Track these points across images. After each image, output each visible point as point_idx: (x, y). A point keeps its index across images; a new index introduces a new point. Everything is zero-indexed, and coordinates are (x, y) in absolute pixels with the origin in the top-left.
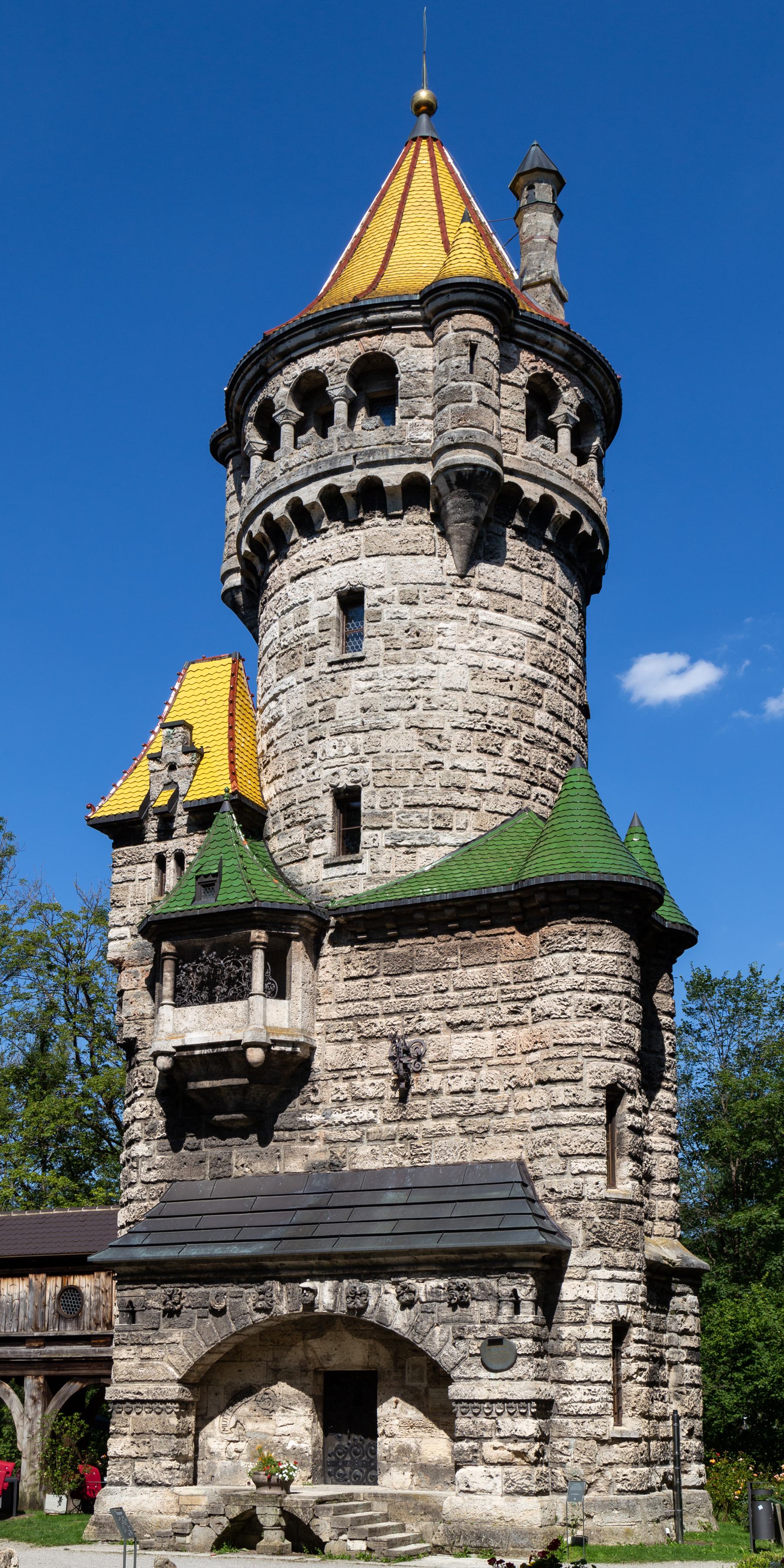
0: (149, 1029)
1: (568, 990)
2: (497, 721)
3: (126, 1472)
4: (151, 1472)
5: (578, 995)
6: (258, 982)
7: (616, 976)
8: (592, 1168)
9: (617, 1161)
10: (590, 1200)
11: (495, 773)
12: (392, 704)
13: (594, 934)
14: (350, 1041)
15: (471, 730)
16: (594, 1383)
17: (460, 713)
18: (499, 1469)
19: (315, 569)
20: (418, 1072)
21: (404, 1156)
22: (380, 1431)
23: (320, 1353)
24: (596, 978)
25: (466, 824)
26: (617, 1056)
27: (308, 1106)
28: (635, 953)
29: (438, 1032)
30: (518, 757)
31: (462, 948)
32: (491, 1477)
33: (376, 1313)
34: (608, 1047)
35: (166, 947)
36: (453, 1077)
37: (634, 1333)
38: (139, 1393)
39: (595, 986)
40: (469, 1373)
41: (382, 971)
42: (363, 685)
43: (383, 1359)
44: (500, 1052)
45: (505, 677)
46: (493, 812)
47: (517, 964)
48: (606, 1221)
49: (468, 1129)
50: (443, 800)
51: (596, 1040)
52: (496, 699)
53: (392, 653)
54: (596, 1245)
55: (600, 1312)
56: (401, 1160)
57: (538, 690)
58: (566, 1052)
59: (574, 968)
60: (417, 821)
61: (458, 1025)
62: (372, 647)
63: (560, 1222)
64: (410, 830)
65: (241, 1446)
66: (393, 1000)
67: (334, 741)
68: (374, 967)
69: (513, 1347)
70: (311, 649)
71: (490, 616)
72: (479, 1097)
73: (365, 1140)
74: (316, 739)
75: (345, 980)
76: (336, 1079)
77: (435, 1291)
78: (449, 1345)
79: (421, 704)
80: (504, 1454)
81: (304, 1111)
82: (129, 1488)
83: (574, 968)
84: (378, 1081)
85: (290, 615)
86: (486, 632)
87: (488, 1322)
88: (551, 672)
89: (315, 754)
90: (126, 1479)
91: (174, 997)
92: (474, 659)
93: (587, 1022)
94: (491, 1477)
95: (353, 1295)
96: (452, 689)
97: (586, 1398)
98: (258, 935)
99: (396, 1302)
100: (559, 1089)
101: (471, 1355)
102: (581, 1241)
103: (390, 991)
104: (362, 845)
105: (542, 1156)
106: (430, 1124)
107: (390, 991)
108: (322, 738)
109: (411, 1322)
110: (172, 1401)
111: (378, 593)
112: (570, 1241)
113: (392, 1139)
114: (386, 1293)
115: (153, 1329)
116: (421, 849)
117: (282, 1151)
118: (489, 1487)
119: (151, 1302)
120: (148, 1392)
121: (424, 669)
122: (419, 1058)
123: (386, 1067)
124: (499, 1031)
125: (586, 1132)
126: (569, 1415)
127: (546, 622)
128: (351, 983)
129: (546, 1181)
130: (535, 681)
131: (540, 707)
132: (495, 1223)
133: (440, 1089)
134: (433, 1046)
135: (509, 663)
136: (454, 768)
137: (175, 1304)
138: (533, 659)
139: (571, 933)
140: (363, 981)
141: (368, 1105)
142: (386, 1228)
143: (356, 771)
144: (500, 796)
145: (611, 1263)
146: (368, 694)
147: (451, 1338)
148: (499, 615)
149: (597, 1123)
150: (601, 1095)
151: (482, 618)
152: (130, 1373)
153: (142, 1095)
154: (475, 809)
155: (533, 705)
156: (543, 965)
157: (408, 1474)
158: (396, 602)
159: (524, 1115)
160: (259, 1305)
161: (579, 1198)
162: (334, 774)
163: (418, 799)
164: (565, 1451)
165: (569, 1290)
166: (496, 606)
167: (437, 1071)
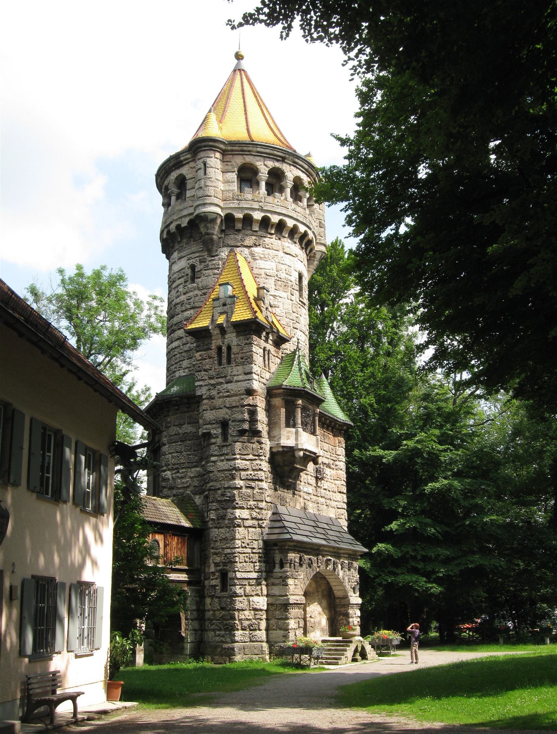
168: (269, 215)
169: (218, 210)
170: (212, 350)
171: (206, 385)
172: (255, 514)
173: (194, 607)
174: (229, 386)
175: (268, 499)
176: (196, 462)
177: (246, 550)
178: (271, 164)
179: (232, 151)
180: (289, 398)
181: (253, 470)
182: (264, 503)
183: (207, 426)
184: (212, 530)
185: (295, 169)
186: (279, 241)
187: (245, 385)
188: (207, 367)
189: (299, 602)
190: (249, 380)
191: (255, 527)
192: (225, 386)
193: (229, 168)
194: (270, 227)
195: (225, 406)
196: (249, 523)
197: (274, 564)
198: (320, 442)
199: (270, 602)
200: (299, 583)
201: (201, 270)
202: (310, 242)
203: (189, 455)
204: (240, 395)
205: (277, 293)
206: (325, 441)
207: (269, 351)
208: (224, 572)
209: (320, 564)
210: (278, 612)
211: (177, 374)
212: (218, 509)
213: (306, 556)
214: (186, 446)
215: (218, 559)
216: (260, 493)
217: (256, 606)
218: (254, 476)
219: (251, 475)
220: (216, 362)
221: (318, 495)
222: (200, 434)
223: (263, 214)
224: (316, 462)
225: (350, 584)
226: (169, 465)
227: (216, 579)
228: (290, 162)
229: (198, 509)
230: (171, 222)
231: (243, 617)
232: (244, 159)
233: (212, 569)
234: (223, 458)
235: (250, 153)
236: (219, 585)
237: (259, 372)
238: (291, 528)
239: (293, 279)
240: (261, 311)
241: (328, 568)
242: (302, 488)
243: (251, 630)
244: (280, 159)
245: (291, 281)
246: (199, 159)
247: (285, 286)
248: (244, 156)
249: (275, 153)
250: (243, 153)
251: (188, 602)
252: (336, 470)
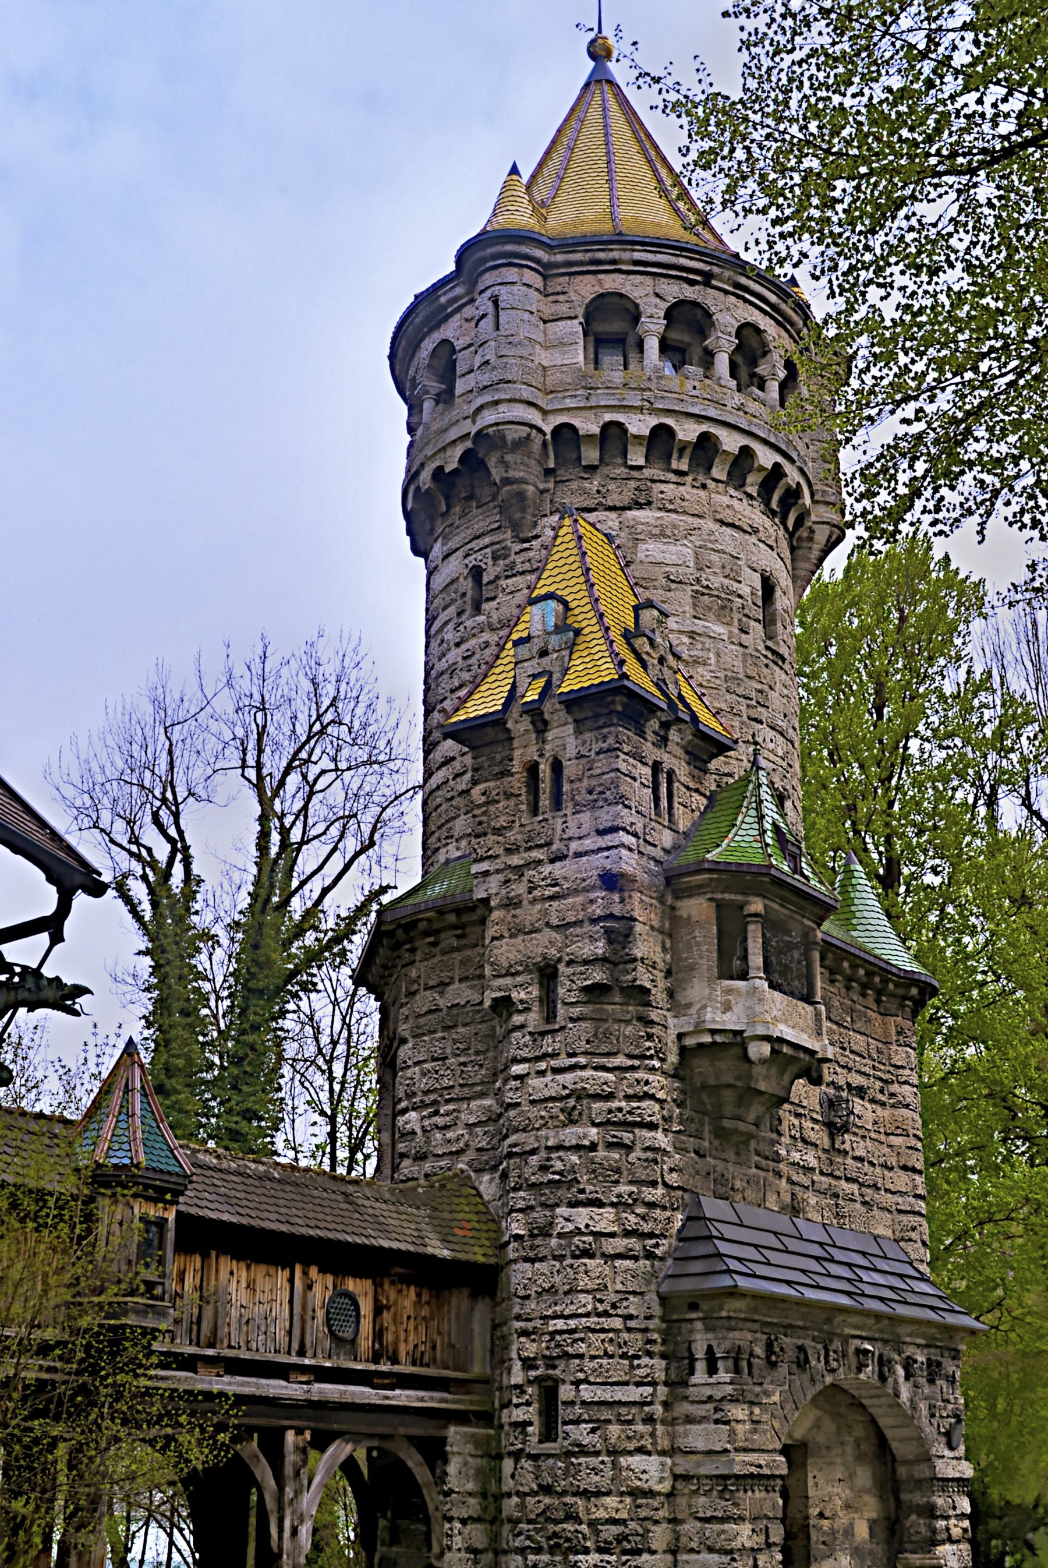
38: (760, 1466)
105: (910, 1240)
168: (670, 421)
169: (534, 416)
170: (512, 775)
171: (498, 871)
172: (633, 1219)
173: (470, 1486)
174: (558, 869)
175: (673, 1179)
176: (482, 1083)
177: (606, 1323)
178: (674, 291)
179: (569, 264)
180: (727, 896)
181: (628, 1098)
182: (660, 1191)
183: (501, 981)
184: (514, 1267)
185: (740, 303)
186: (702, 493)
187: (599, 861)
188: (502, 821)
189: (766, 1471)
190: (608, 848)
191: (636, 1258)
192: (547, 869)
193: (563, 309)
194: (675, 455)
195: (548, 925)
196: (619, 1244)
197: (692, 1360)
198: (826, 1024)
199: (679, 1470)
200: (765, 1417)
201: (497, 578)
202: (793, 495)
203: (464, 1064)
204: (586, 890)
205: (699, 625)
206: (857, 1026)
207: (671, 775)
208: (550, 1383)
209: (835, 1364)
210: (702, 1500)
211: (442, 857)
212: (531, 1208)
213: (788, 1340)
214: (455, 1041)
215: (531, 1349)
216: (646, 1160)
217: (639, 1483)
218: (630, 1113)
219: (620, 1110)
220: (524, 807)
221: (837, 1173)
222: (487, 1003)
223: (653, 421)
224: (817, 1081)
225: (935, 1421)
226: (414, 1094)
227: (528, 1404)
228: (726, 287)
229: (488, 1212)
230: (422, 465)
231: (601, 1514)
232: (600, 281)
233: (517, 1376)
234: (543, 1066)
235: (614, 267)
236: (536, 1423)
237: (639, 828)
238: (739, 1260)
239: (744, 590)
240: (644, 665)
241: (862, 1376)
242: (783, 1152)
243: (625, 1552)
244: (698, 278)
245: (740, 596)
246: (482, 292)
247: (723, 608)
248: (601, 276)
249: (683, 261)
250: (596, 268)
251: (452, 1469)
252: (893, 1106)
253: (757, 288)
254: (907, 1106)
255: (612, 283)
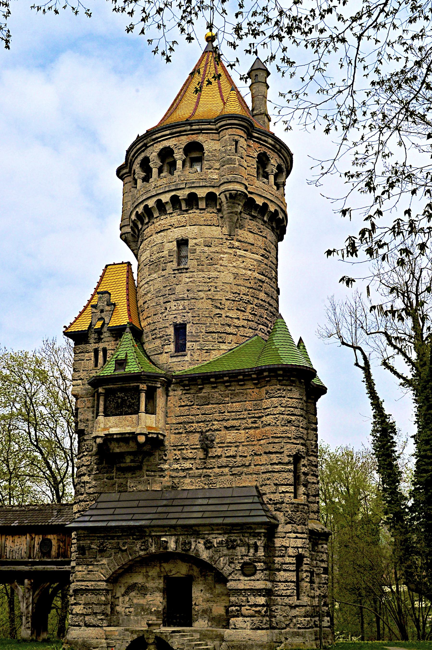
0: (90, 426)
1: (278, 414)
2: (244, 297)
3: (81, 621)
4: (92, 621)
5: (282, 416)
6: (143, 407)
7: (297, 408)
8: (287, 490)
9: (298, 487)
10: (287, 504)
11: (243, 319)
12: (200, 288)
13: (288, 390)
14: (181, 433)
15: (234, 301)
16: (288, 582)
17: (229, 293)
18: (248, 619)
19: (167, 229)
20: (212, 448)
21: (205, 484)
22: (193, 603)
23: (167, 569)
24: (289, 409)
25: (232, 341)
26: (298, 442)
27: (162, 461)
28: (305, 398)
29: (220, 430)
30: (253, 312)
31: (231, 395)
32: (245, 622)
33: (195, 551)
34: (294, 438)
35: (100, 390)
36: (227, 450)
37: (305, 561)
39: (289, 412)
40: (236, 577)
41: (196, 403)
42: (188, 280)
43: (196, 572)
44: (248, 440)
45: (247, 278)
46: (243, 336)
47: (255, 402)
48: (294, 513)
49: (234, 472)
50: (222, 330)
51: (290, 435)
52: (244, 288)
53: (200, 267)
54: (289, 523)
55: (291, 551)
56: (204, 485)
57: (261, 284)
58: (277, 440)
59: (280, 405)
60: (211, 339)
61: (229, 428)
62: (191, 264)
63: (274, 513)
64: (207, 343)
65: (132, 610)
66: (200, 416)
67: (173, 303)
68: (192, 402)
69: (255, 567)
70: (165, 263)
71: (242, 253)
72: (238, 459)
73: (188, 476)
74: (167, 302)
75: (179, 407)
76: (175, 450)
77: (221, 543)
78: (227, 565)
79: (213, 289)
80: (251, 612)
81: (161, 463)
82: (82, 628)
83: (280, 405)
84: (194, 451)
85: (155, 248)
86: (240, 259)
87: (244, 555)
88: (266, 276)
89: (166, 309)
90: (81, 624)
91: (104, 412)
92: (235, 270)
93: (286, 428)
94: (245, 622)
95: (184, 544)
96: (225, 283)
97: (285, 588)
98: (143, 387)
99: (203, 547)
100: (273, 456)
101: (236, 570)
102: (283, 521)
103: (199, 412)
104: (187, 348)
105: (266, 484)
106: (217, 470)
107: (199, 412)
108: (169, 302)
109: (210, 555)
110: (103, 590)
111: (194, 241)
112: (278, 521)
113: (200, 476)
114: (199, 543)
115: (93, 558)
116: (212, 351)
117: (150, 481)
118: (245, 626)
119: (93, 546)
120: (91, 586)
121: (214, 274)
122: (212, 441)
123: (197, 445)
124: (247, 431)
125: (285, 475)
126: (279, 596)
127: (264, 255)
128: (182, 408)
129: (268, 495)
130: (260, 280)
131: (262, 291)
132: (247, 513)
133: (221, 455)
134: (218, 437)
135: (249, 273)
136: (227, 317)
137: (104, 547)
138: (259, 271)
139: (279, 390)
140: (187, 407)
141: (189, 461)
142: (200, 515)
143: (184, 316)
144: (245, 329)
145: (296, 531)
146: (190, 284)
147: (228, 563)
148: (245, 252)
149: (289, 471)
150: (291, 459)
151: (238, 253)
152: (83, 577)
153: (87, 455)
154: (235, 335)
155: (259, 290)
156: (267, 403)
157: (206, 622)
158: (202, 245)
159: (258, 467)
160: (142, 548)
161: (283, 502)
162: (175, 317)
163: (211, 330)
164: (276, 611)
165: (278, 542)
166: (244, 248)
167: (220, 447)
249: (138, 147)
253: (160, 135)
254: (269, 425)
255: (194, 138)
